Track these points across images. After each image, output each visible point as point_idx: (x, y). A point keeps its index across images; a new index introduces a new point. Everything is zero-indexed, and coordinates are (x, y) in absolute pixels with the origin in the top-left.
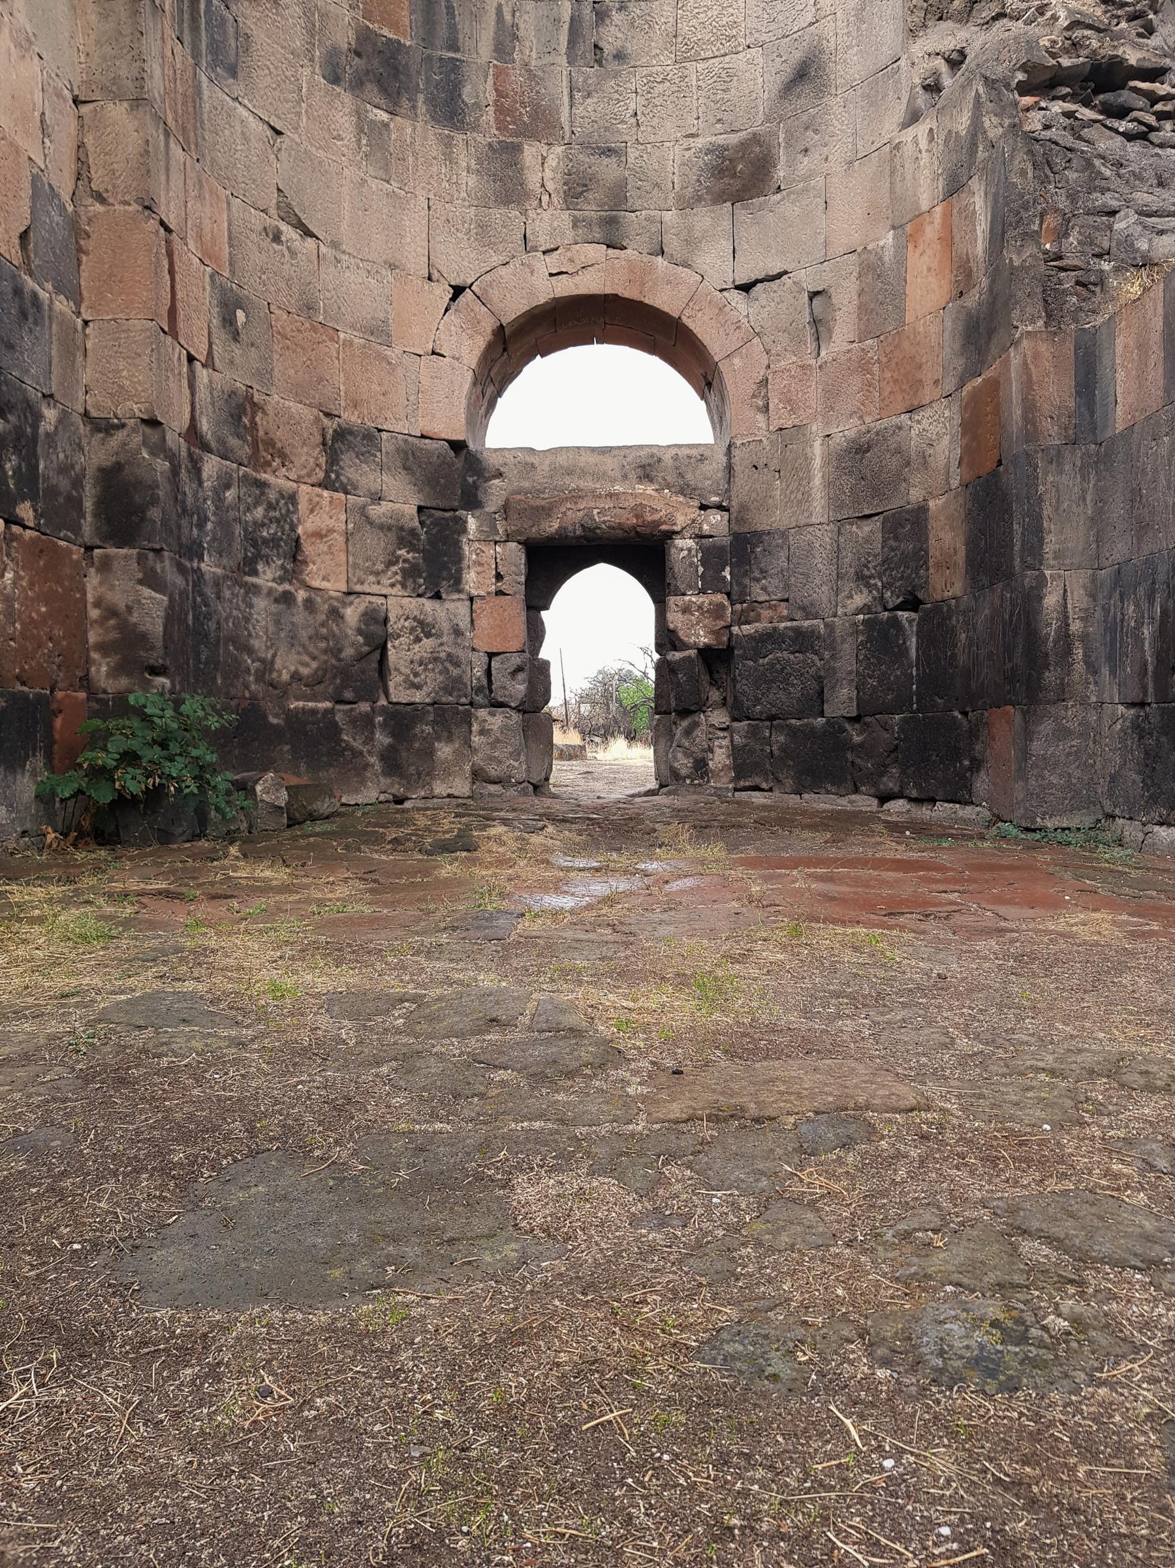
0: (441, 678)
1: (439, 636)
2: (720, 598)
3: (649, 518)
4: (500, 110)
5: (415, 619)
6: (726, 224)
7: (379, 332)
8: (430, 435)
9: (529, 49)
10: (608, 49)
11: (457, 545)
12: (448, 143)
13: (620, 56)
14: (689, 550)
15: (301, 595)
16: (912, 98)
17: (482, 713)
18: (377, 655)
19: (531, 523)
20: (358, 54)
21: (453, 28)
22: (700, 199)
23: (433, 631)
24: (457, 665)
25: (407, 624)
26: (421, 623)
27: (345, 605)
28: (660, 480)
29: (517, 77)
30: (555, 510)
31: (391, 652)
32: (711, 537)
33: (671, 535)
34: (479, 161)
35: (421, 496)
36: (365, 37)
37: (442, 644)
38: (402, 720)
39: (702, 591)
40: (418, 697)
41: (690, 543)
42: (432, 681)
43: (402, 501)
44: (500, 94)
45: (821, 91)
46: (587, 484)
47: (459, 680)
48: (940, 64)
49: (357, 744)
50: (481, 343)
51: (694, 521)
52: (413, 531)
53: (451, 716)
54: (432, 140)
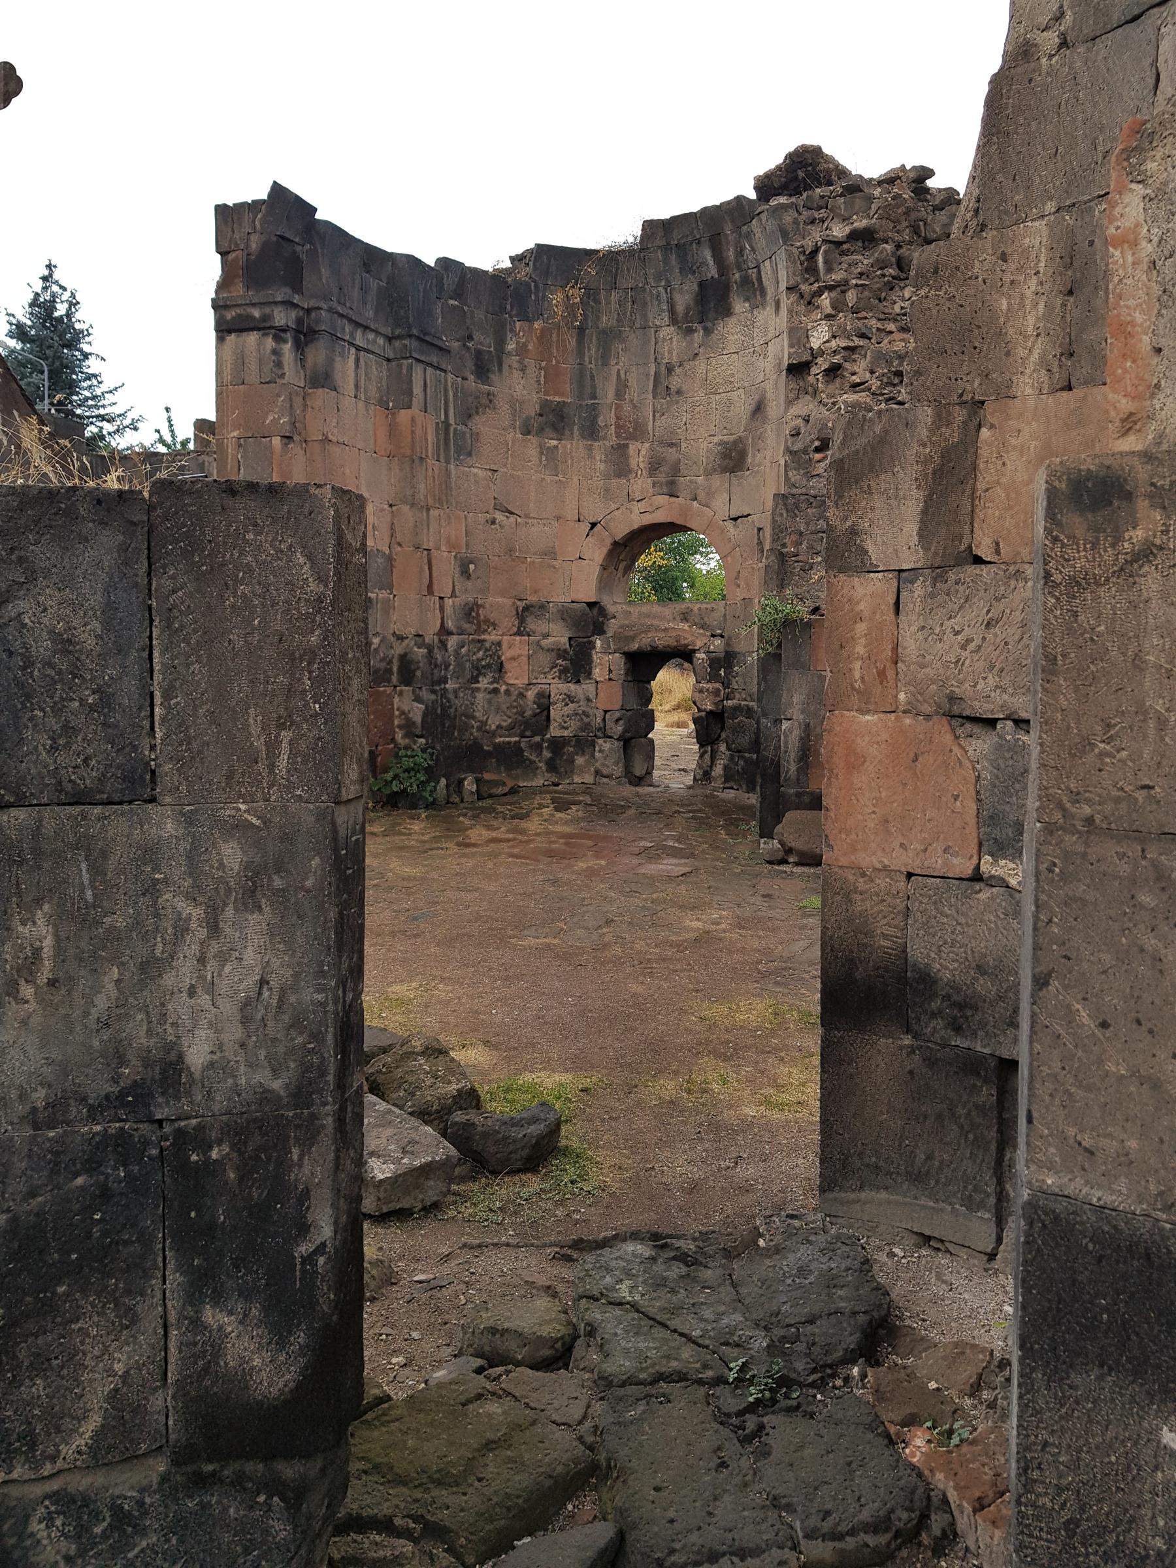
0: (579, 724)
2: (718, 685)
3: (683, 642)
4: (618, 426)
6: (727, 485)
7: (550, 553)
9: (633, 393)
10: (673, 389)
11: (590, 655)
12: (589, 448)
13: (679, 392)
15: (504, 687)
16: (786, 441)
17: (600, 741)
18: (545, 713)
20: (541, 415)
21: (594, 387)
22: (715, 470)
24: (588, 716)
26: (569, 696)
27: (527, 690)
29: (627, 408)
31: (552, 711)
33: (694, 651)
34: (607, 456)
36: (545, 404)
38: (557, 745)
39: (709, 681)
40: (566, 733)
41: (703, 656)
42: (574, 725)
43: (560, 636)
44: (618, 418)
45: (764, 420)
46: (656, 622)
47: (589, 724)
48: (799, 421)
49: (533, 758)
50: (605, 550)
52: (565, 651)
53: (584, 742)
54: (581, 449)
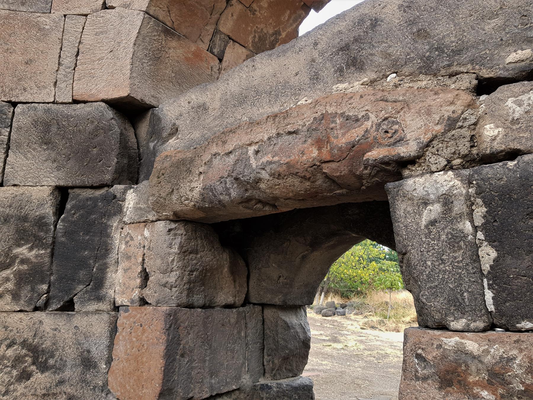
1: (58, 369)
3: (342, 139)
5: (24, 344)
8: (86, 98)
11: (104, 233)
14: (447, 200)
19: (168, 188)
23: (51, 362)
25: (10, 352)
28: (378, 59)
30: (198, 162)
32: (513, 154)
35: (61, 174)
37: (61, 382)
41: (447, 181)
51: (452, 123)
